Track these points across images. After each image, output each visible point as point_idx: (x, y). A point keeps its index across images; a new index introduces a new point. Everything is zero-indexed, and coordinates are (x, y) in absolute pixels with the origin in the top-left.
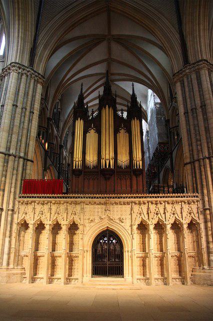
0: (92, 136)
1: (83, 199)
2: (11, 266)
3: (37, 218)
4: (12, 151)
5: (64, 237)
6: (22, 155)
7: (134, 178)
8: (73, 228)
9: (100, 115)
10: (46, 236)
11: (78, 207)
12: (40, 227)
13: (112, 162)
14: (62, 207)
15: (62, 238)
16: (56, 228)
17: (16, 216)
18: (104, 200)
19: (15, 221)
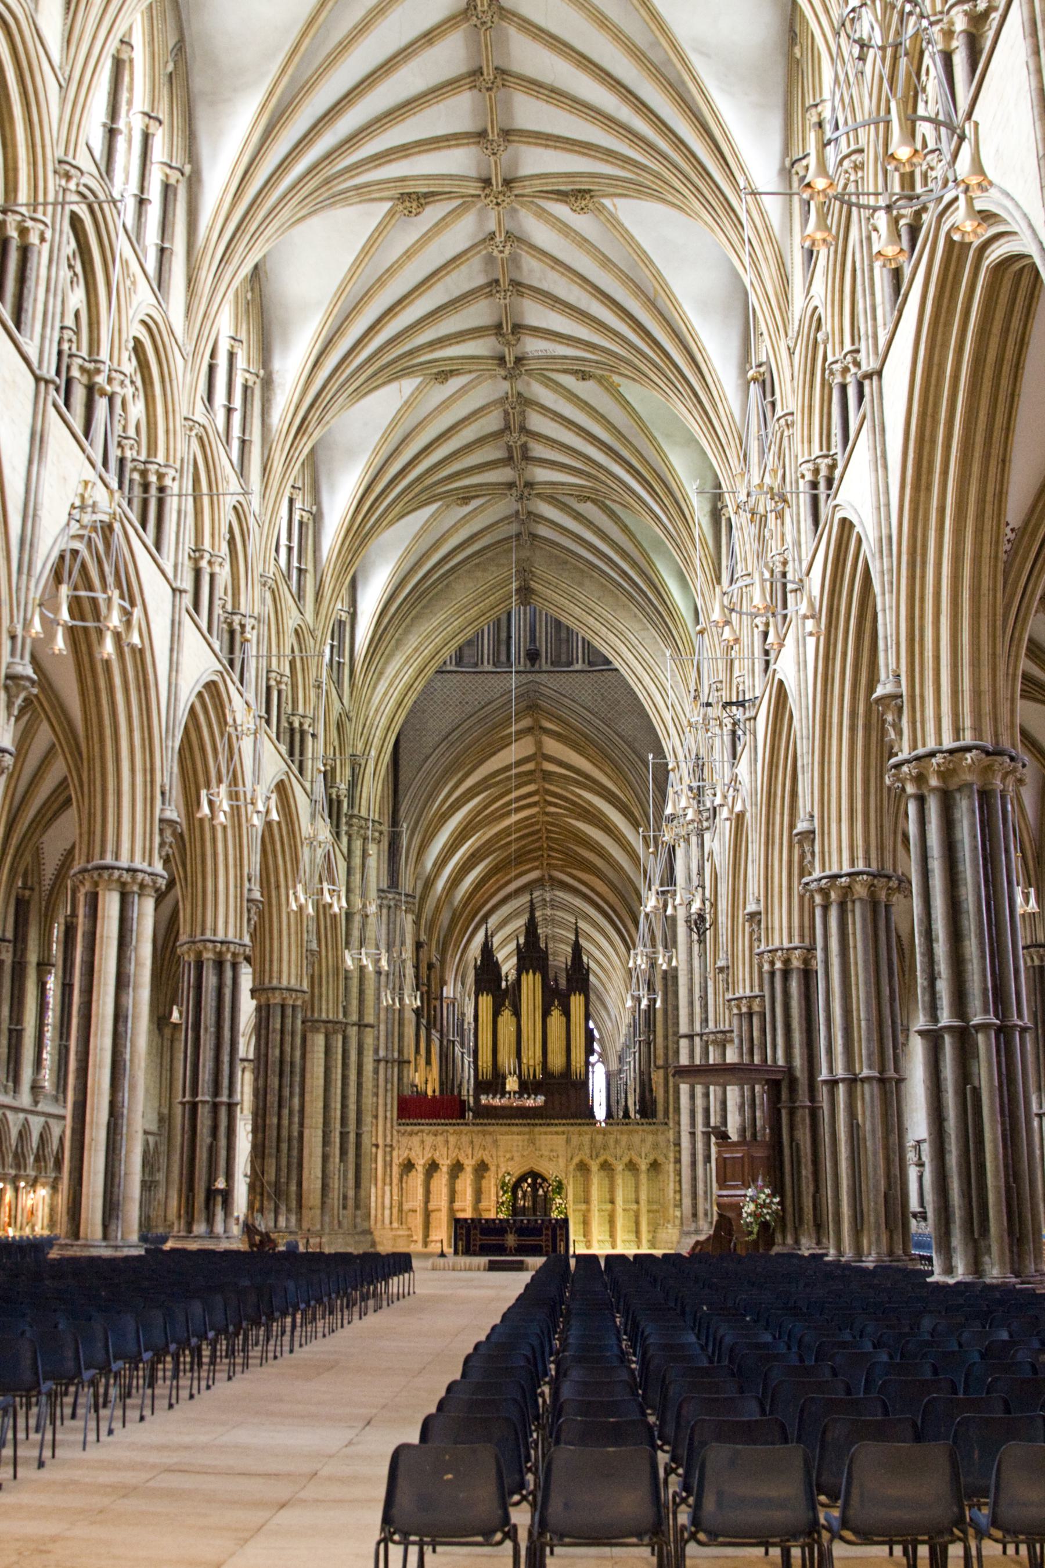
0: (506, 1017)
1: (496, 1128)
2: (395, 1225)
3: (428, 1155)
4: (382, 1053)
5: (469, 1182)
6: (396, 1055)
7: (572, 1092)
8: (482, 1168)
9: (518, 981)
10: (442, 1181)
11: (489, 1139)
12: (433, 1167)
13: (538, 1069)
14: (465, 1139)
15: (466, 1183)
16: (457, 1168)
17: (395, 1153)
18: (526, 1129)
19: (396, 1161)
